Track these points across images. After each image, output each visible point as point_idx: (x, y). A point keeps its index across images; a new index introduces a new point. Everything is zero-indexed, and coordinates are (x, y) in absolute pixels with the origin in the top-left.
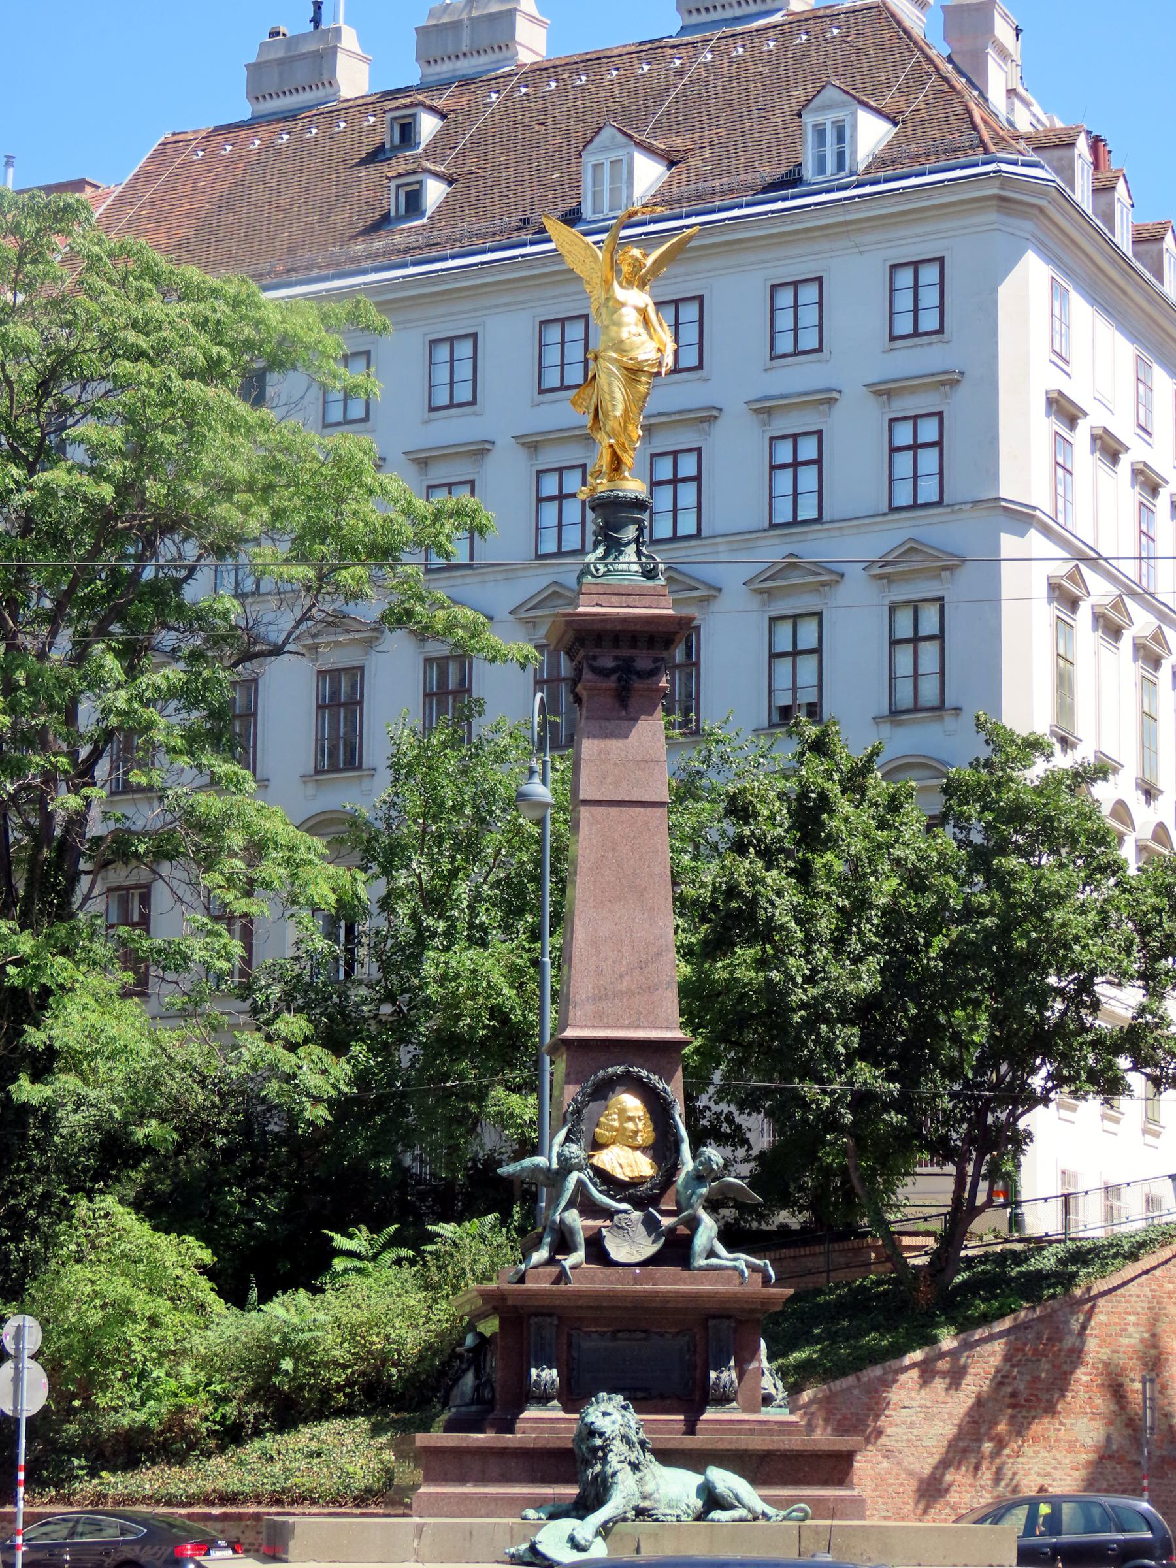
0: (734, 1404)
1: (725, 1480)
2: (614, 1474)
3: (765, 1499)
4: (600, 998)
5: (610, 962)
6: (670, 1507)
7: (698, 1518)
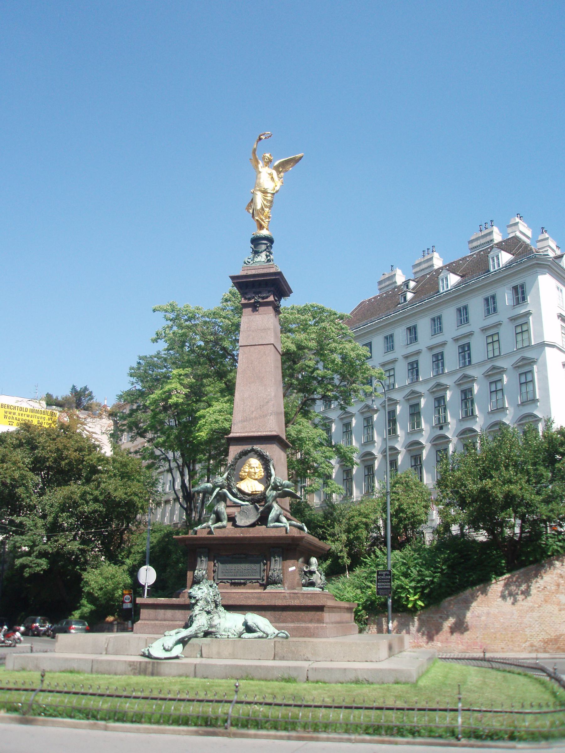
0: (279, 585)
1: (254, 618)
2: (195, 616)
5: (248, 407)
6: (225, 631)
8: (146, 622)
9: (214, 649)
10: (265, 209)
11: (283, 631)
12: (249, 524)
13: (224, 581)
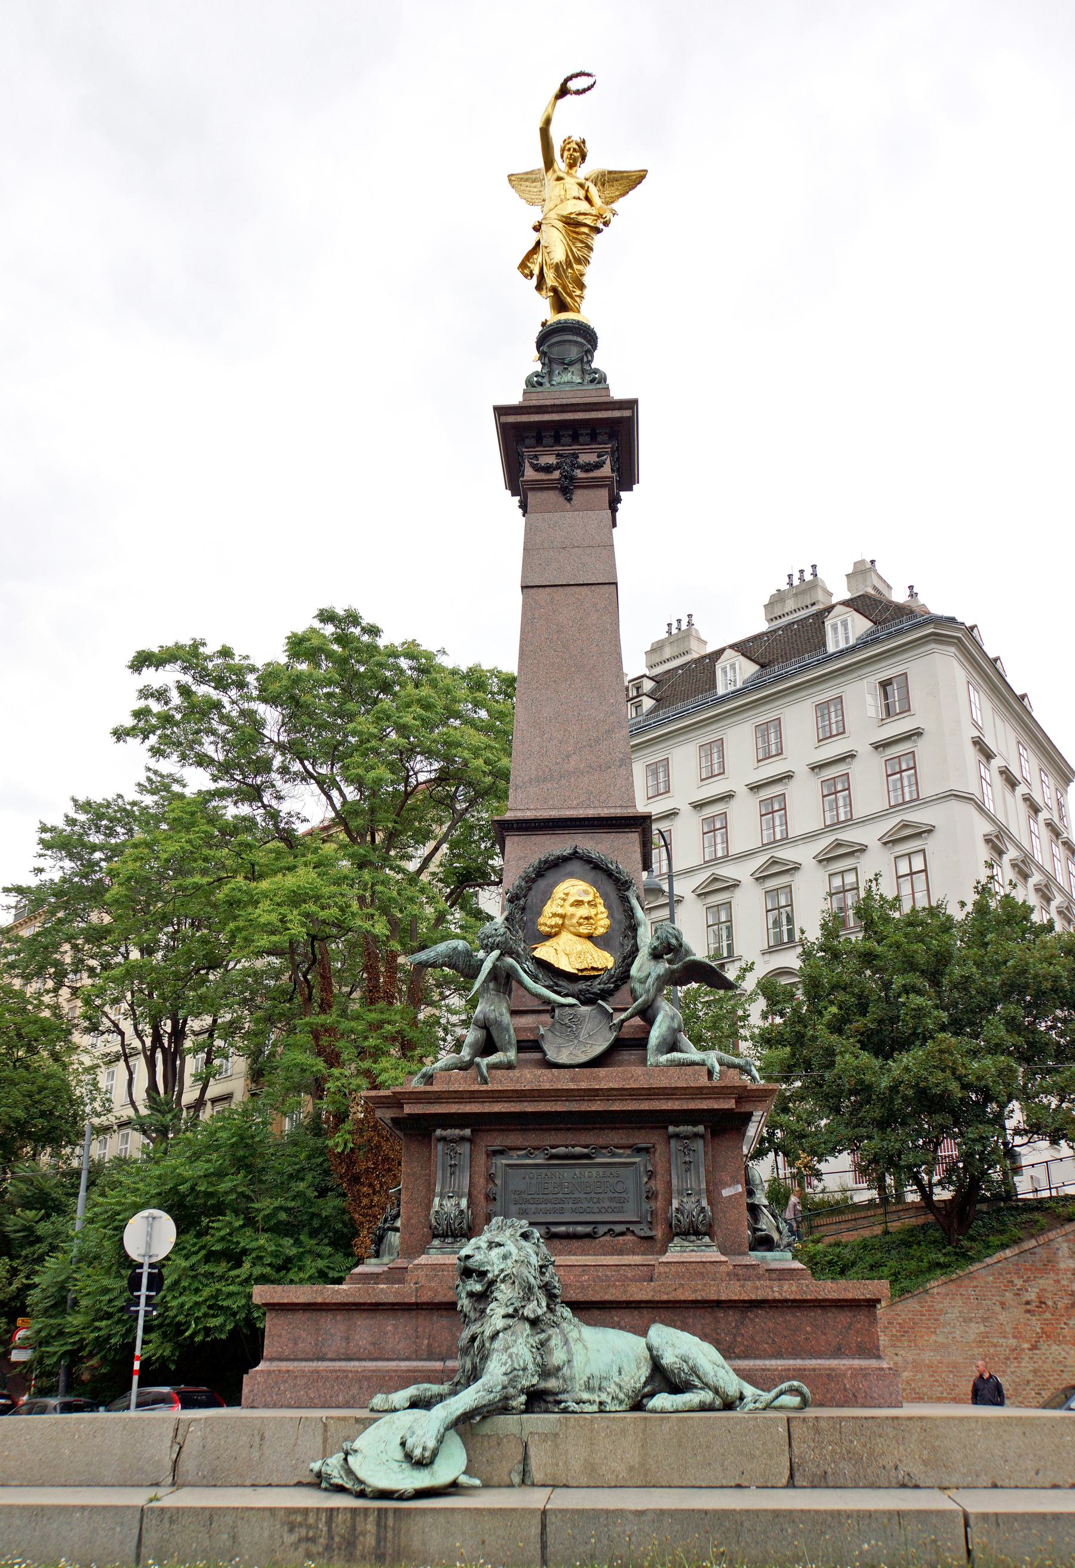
0: (707, 1239)
1: (678, 1345)
2: (494, 1336)
3: (744, 1375)
4: (545, 780)
6: (589, 1388)
7: (638, 1406)
8: (284, 1365)
9: (575, 1454)
11: (784, 1386)
12: (583, 1058)
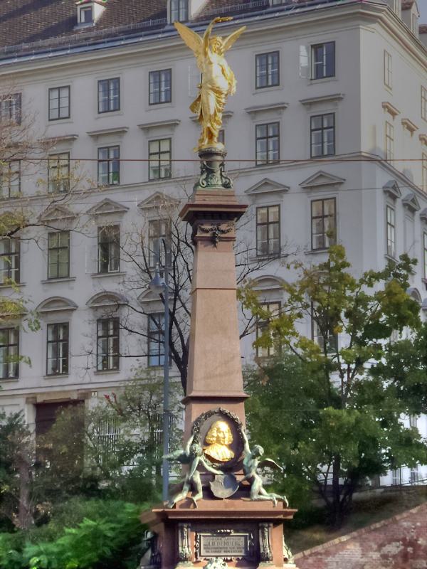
0: (271, 562)
10: (218, 114)
13: (207, 558)
